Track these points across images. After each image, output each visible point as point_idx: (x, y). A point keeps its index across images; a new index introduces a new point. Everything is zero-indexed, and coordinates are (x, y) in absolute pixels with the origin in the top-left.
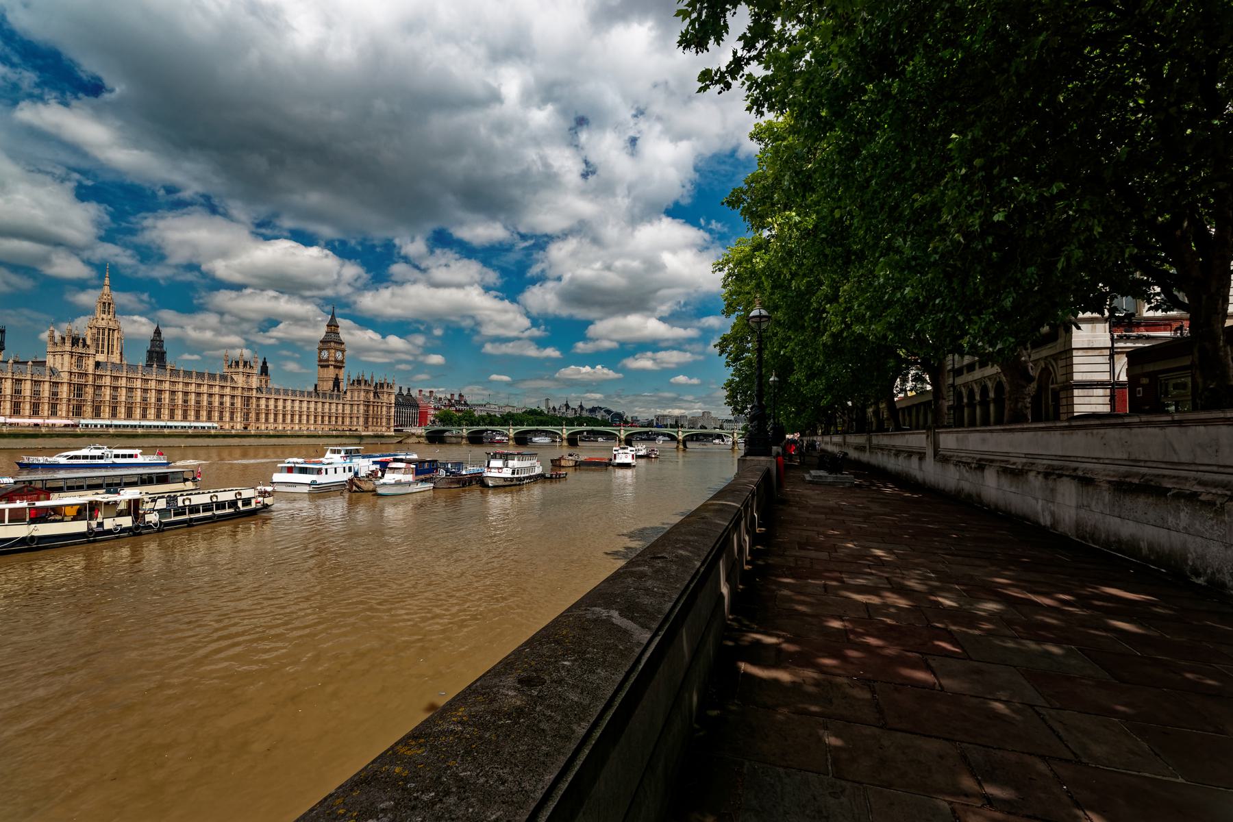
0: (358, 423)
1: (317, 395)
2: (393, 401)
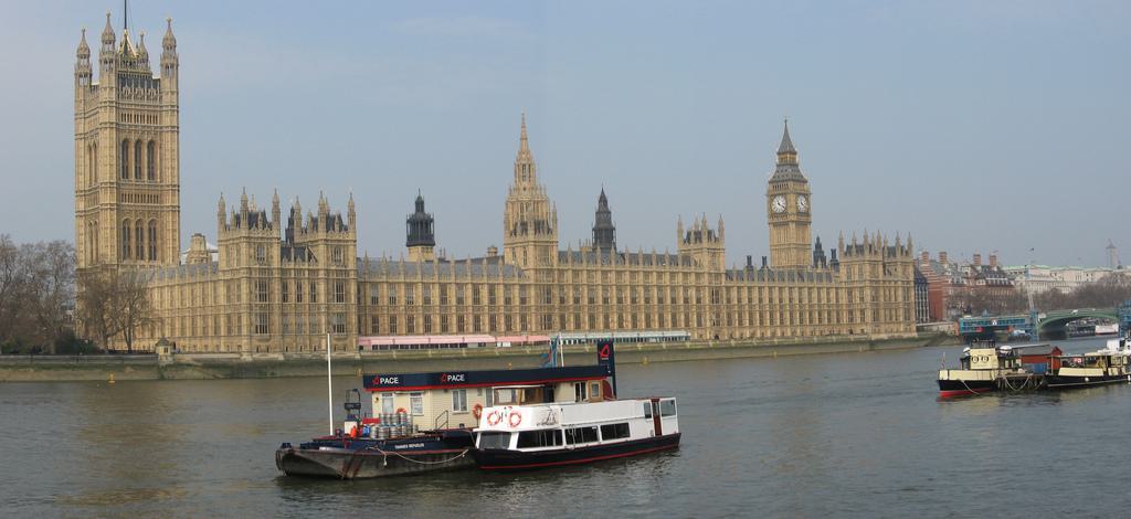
0: (863, 319)
1: (801, 277)
2: (912, 278)
